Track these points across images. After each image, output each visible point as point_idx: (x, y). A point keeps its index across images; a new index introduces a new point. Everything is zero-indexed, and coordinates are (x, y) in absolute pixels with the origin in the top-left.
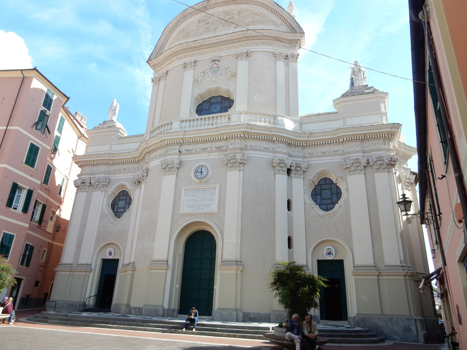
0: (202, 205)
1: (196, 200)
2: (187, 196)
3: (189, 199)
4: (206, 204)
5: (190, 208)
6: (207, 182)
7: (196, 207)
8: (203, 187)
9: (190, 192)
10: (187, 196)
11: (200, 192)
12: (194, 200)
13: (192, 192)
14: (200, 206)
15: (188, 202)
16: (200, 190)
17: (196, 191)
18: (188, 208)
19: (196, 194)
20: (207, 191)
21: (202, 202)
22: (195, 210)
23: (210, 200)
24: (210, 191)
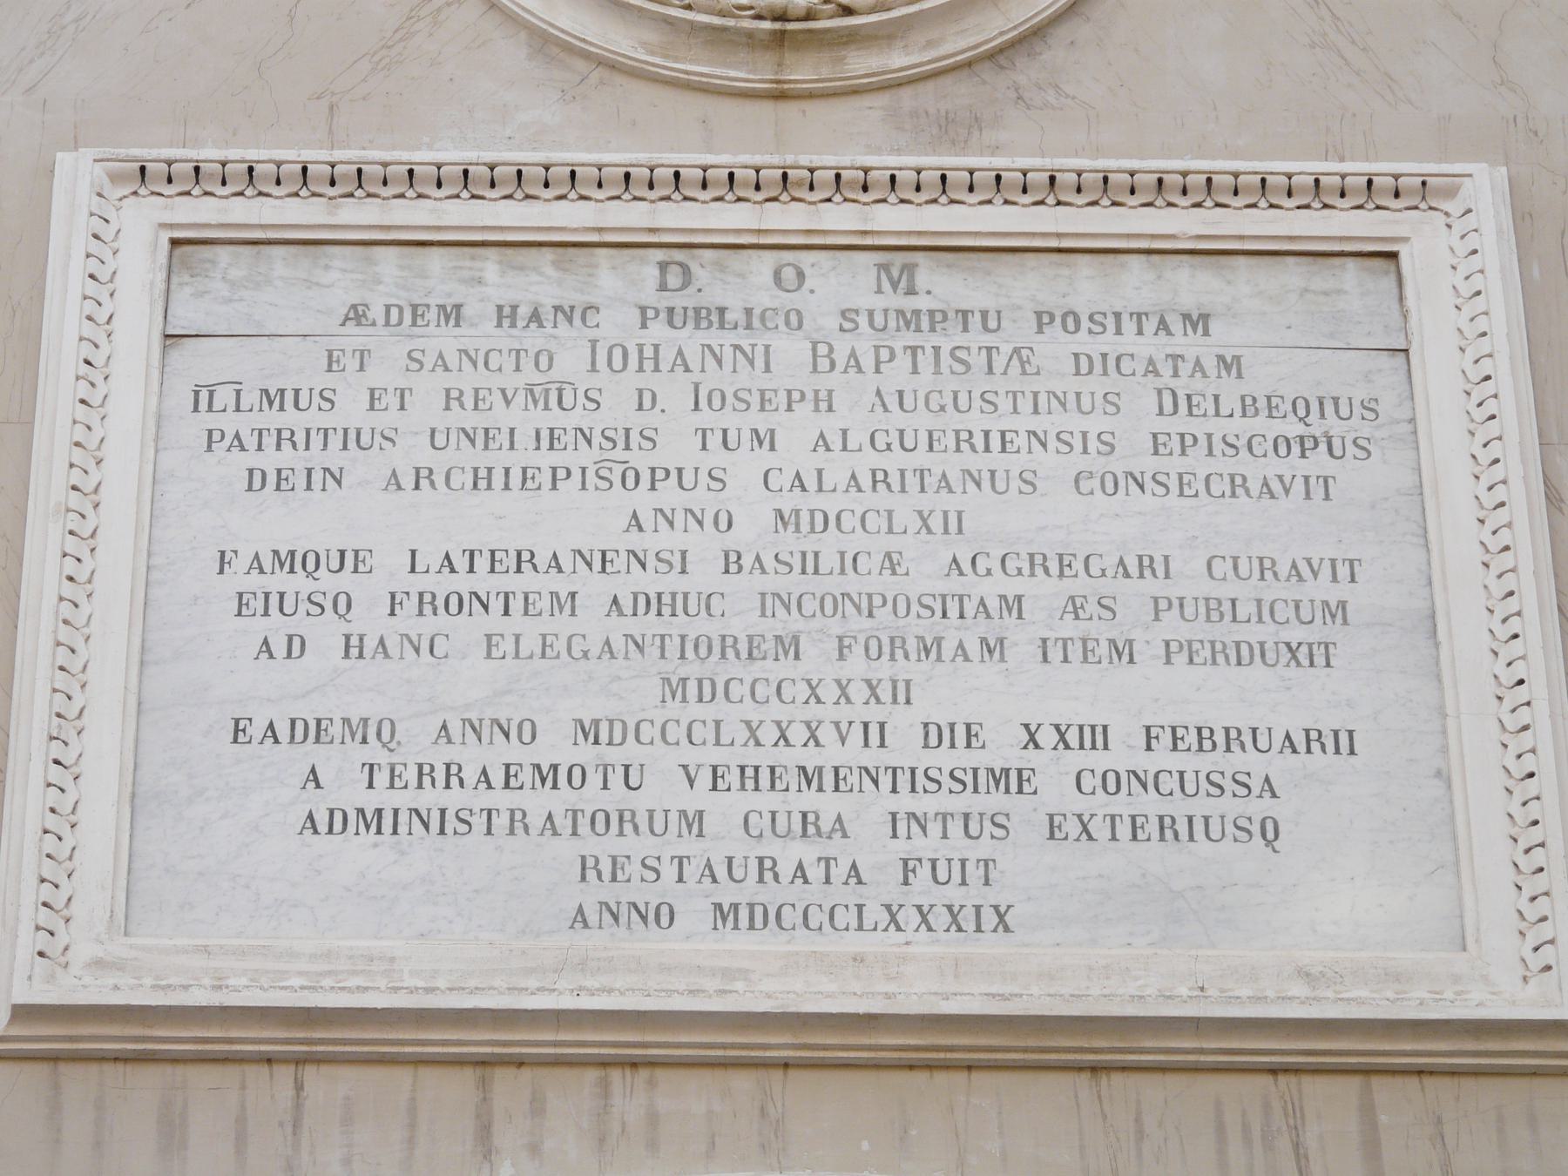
0: (905, 749)
1: (653, 603)
2: (270, 460)
3: (351, 560)
4: (1097, 737)
5: (421, 847)
6: (1026, 72)
7: (694, 822)
8: (892, 219)
9: (354, 337)
10: (270, 460)
11: (790, 350)
12: (594, 588)
13: (482, 333)
14: (827, 805)
15: (325, 633)
16: (764, 296)
17: (616, 324)
18: (358, 849)
19: (645, 401)
20: (1055, 348)
21: (904, 669)
22: (662, 916)
23: (1212, 609)
24: (1186, 343)
